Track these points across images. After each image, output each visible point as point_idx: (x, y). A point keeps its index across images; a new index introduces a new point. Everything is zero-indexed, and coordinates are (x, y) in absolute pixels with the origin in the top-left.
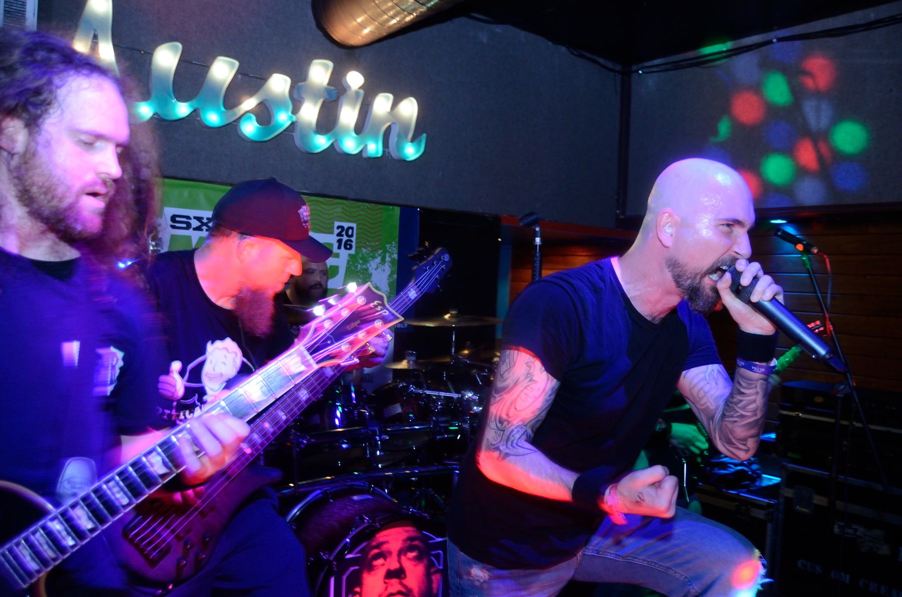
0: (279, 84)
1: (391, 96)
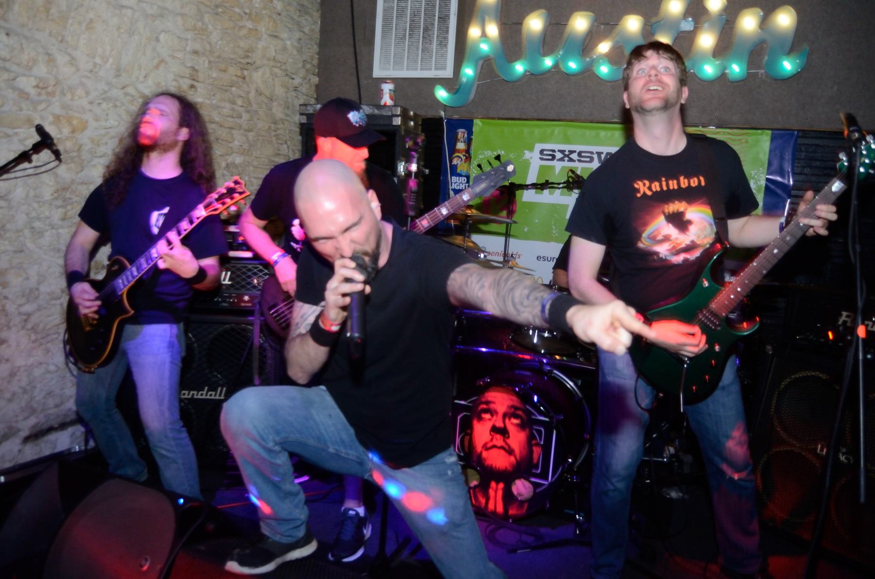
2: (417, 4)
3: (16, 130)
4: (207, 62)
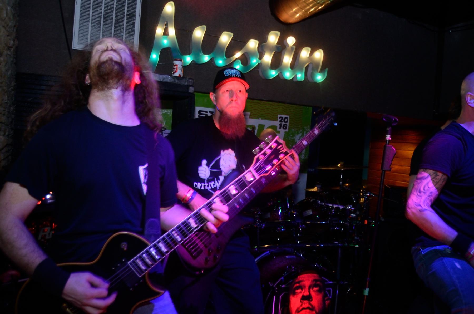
0: (253, 44)
1: (310, 49)
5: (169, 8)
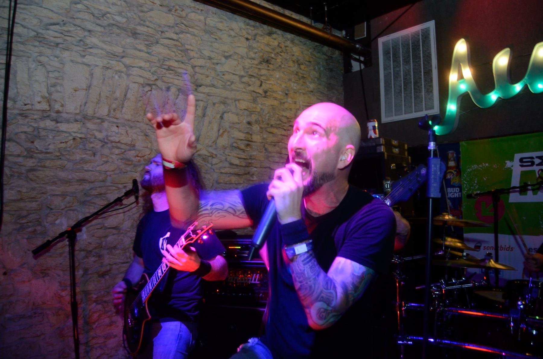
2: (407, 67)
3: (125, 185)
4: (259, 128)
5: (461, 47)
